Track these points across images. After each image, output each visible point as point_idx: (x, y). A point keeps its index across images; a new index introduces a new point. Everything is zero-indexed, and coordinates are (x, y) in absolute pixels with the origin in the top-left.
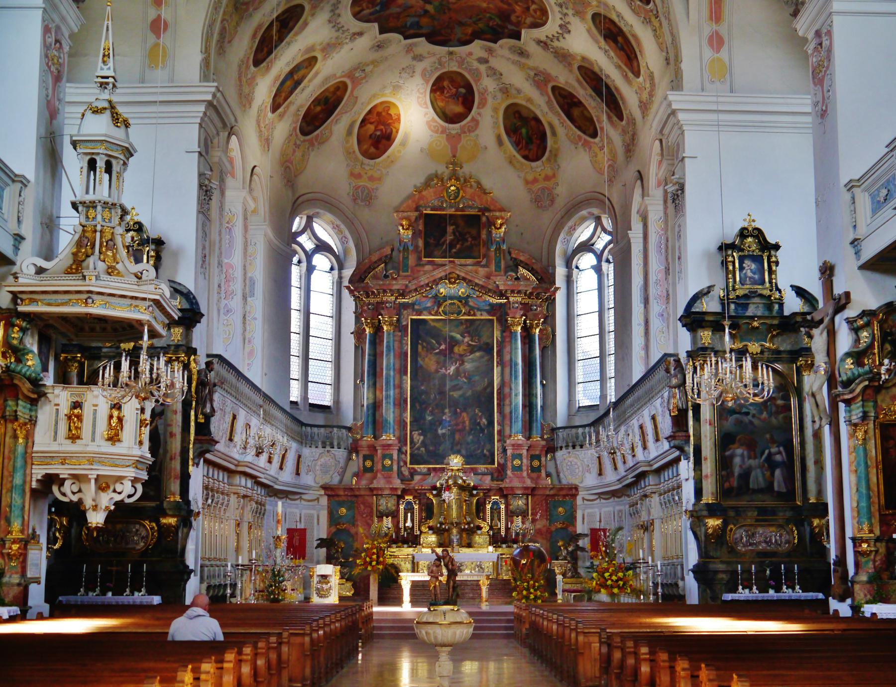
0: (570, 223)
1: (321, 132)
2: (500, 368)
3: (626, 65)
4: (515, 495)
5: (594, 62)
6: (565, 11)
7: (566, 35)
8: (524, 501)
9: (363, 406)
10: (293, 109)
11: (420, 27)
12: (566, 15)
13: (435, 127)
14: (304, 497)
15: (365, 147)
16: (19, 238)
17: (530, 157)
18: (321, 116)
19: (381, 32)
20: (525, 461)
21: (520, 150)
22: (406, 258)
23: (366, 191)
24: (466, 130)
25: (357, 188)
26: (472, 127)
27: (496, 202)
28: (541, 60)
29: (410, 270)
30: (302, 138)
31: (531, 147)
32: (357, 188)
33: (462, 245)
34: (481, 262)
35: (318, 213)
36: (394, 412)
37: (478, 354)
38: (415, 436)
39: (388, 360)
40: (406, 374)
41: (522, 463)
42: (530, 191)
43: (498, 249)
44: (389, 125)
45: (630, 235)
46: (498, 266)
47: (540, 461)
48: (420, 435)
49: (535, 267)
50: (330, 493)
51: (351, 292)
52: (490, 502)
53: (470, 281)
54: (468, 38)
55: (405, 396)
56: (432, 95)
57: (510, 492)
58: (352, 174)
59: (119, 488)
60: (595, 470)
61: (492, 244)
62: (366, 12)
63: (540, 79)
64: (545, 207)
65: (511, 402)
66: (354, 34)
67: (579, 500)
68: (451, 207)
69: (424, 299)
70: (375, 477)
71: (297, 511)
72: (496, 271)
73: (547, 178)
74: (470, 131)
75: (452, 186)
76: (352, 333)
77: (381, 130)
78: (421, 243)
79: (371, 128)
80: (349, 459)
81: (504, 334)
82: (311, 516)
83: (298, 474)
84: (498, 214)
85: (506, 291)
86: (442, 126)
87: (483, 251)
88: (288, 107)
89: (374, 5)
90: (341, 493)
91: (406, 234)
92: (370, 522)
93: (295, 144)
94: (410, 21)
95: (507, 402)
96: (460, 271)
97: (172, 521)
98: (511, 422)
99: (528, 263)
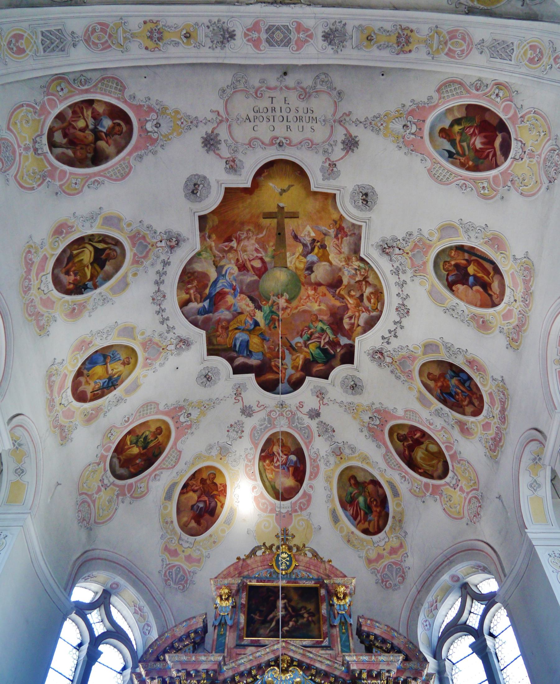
1: (136, 482)
3: (483, 305)
5: (439, 342)
11: (250, 354)
12: (405, 282)
13: (263, 504)
15: (185, 519)
17: (371, 530)
18: (138, 462)
21: (358, 524)
22: (221, 636)
23: (182, 573)
24: (297, 508)
26: (304, 505)
27: (336, 569)
29: (226, 650)
30: (112, 479)
31: (370, 517)
33: (296, 622)
34: (322, 642)
35: (117, 584)
42: (375, 572)
44: (214, 497)
45: (530, 536)
49: (395, 642)
54: (298, 375)
56: (261, 463)
58: (166, 549)
61: (335, 618)
62: (194, 306)
64: (395, 585)
68: (282, 579)
72: (342, 651)
73: (393, 551)
74: (301, 509)
75: (282, 553)
77: (205, 502)
78: (242, 619)
84: (339, 580)
85: (360, 673)
86: (271, 504)
87: (325, 628)
89: (203, 300)
93: (102, 481)
94: (241, 336)
96: (294, 652)
99: (384, 636)
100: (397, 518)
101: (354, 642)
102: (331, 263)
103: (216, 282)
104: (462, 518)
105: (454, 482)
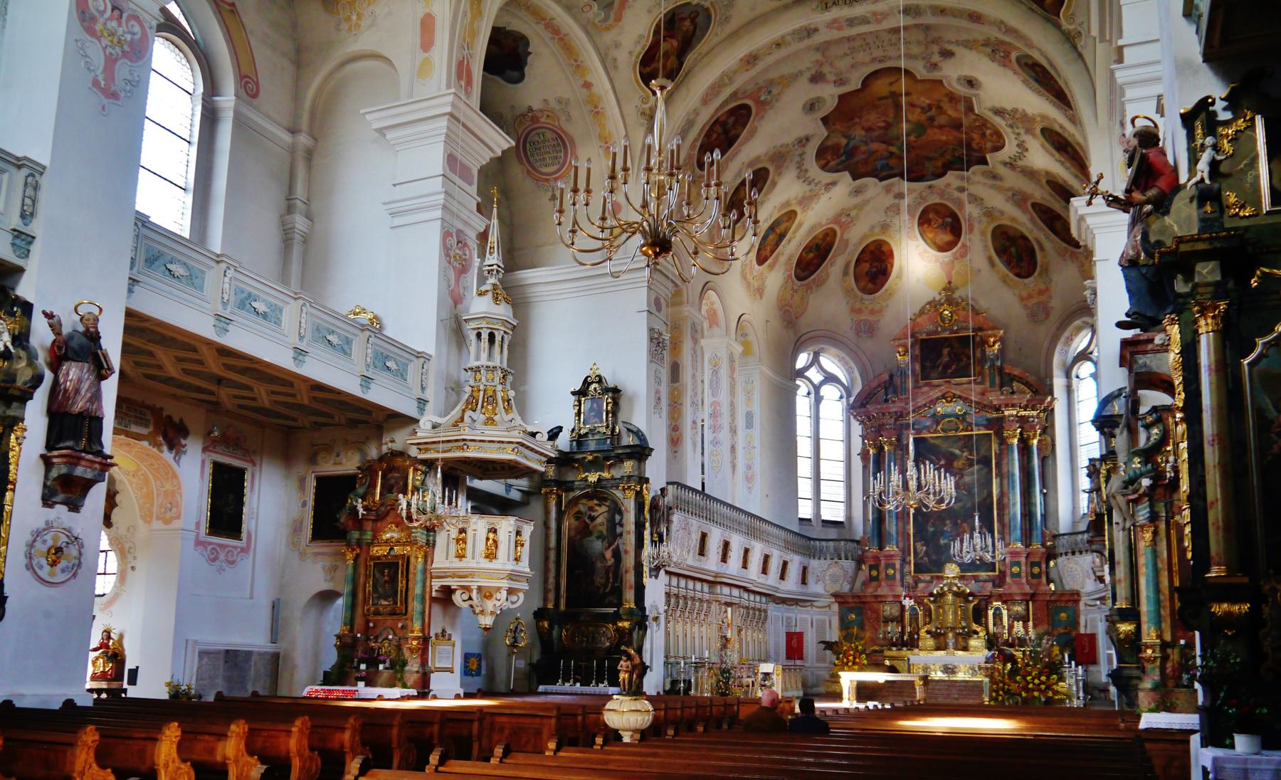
0: (1067, 334)
6: (1017, 131)
7: (1026, 154)
10: (783, 259)
11: (892, 168)
12: (1018, 134)
14: (815, 604)
16: (422, 402)
19: (854, 179)
25: (858, 322)
28: (1012, 180)
30: (799, 283)
31: (1023, 264)
32: (858, 322)
36: (897, 525)
42: (1026, 307)
43: (992, 366)
44: (883, 261)
46: (992, 384)
48: (923, 545)
49: (1029, 380)
51: (855, 417)
53: (966, 399)
59: (498, 595)
62: (833, 163)
63: (1019, 199)
66: (828, 185)
69: (923, 419)
70: (879, 586)
71: (809, 618)
73: (1041, 293)
78: (918, 367)
79: (866, 266)
80: (858, 568)
82: (823, 622)
83: (804, 581)
84: (990, 332)
85: (1000, 406)
88: (777, 258)
90: (850, 600)
91: (904, 360)
93: (793, 289)
94: (879, 164)
97: (626, 624)
102: (949, 116)
103: (847, 144)
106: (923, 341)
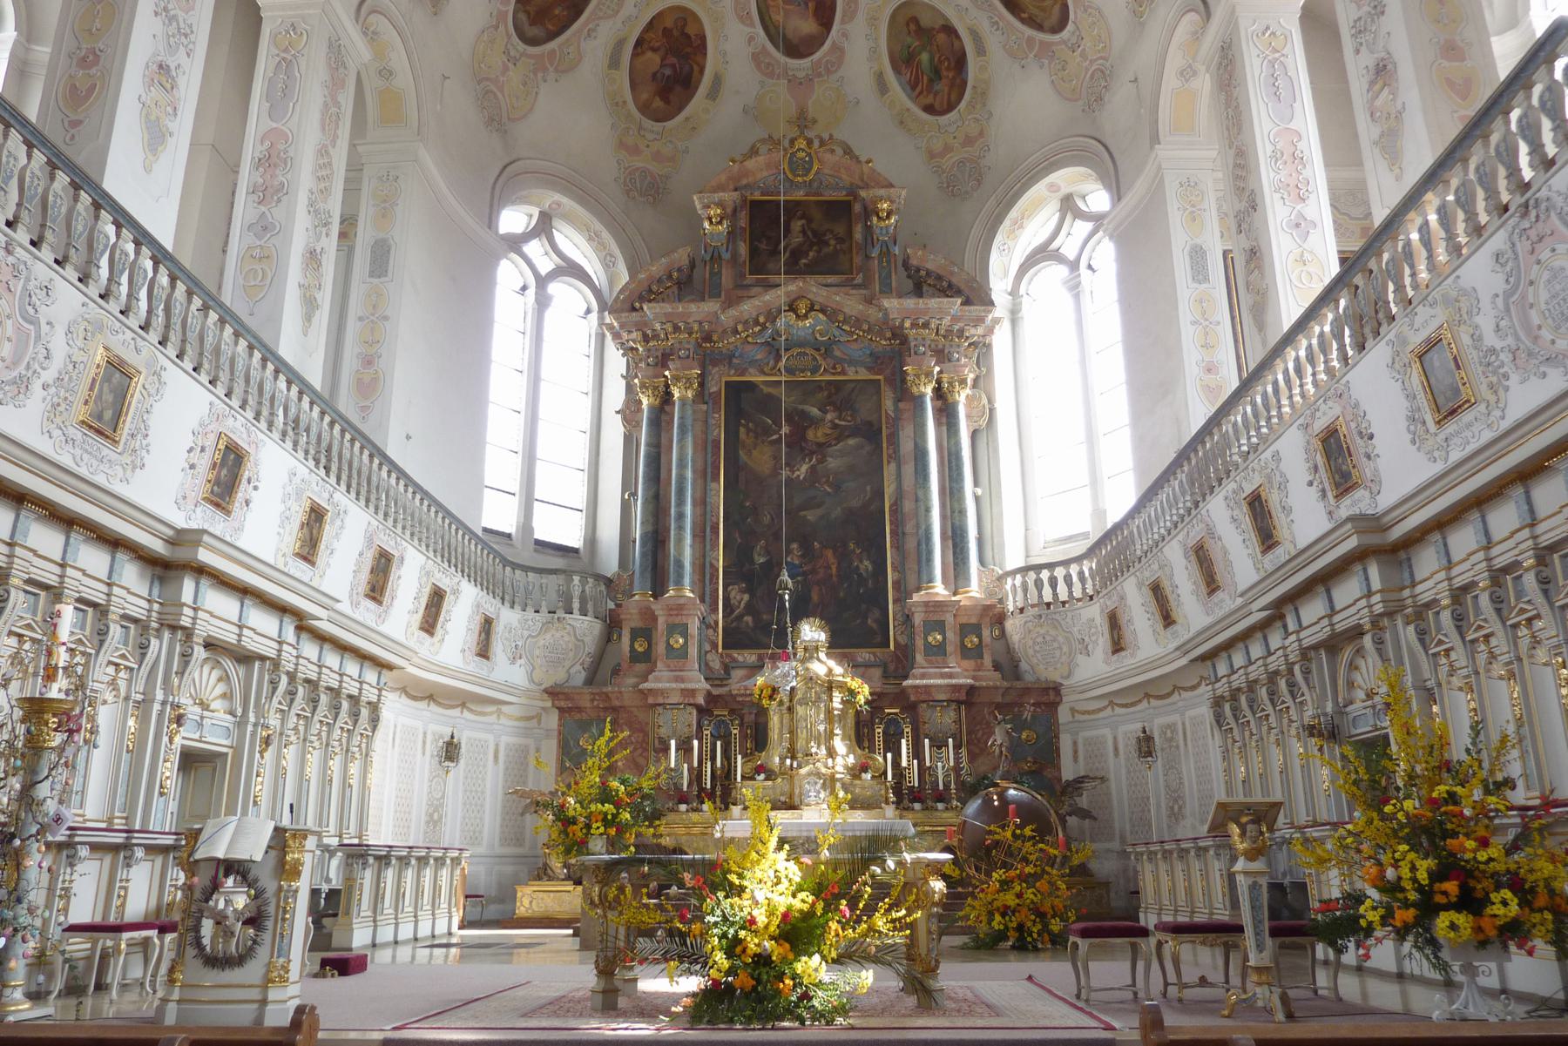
2: (893, 466)
4: (933, 703)
8: (952, 714)
9: (634, 542)
15: (645, 96)
17: (937, 106)
18: (557, 12)
20: (950, 635)
30: (521, 46)
31: (937, 87)
33: (819, 252)
34: (854, 279)
37: (851, 442)
38: (733, 594)
39: (682, 449)
40: (716, 478)
41: (944, 638)
47: (980, 636)
48: (743, 591)
49: (954, 280)
50: (562, 704)
51: (616, 336)
52: (882, 719)
55: (714, 519)
57: (923, 697)
58: (622, 145)
60: (1103, 642)
64: (967, 192)
65: (918, 526)
67: (1063, 714)
69: (748, 348)
71: (491, 738)
73: (969, 141)
74: (829, 72)
76: (618, 412)
77: (673, 66)
78: (743, 249)
81: (901, 405)
83: (484, 652)
84: (882, 192)
87: (858, 260)
92: (641, 761)
95: (909, 528)
98: (919, 562)
100: (979, 91)
101: (898, 278)
104: (1076, 100)
105: (1074, 40)
106: (755, 205)
